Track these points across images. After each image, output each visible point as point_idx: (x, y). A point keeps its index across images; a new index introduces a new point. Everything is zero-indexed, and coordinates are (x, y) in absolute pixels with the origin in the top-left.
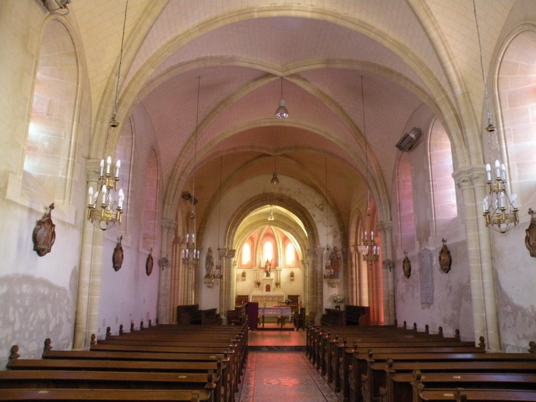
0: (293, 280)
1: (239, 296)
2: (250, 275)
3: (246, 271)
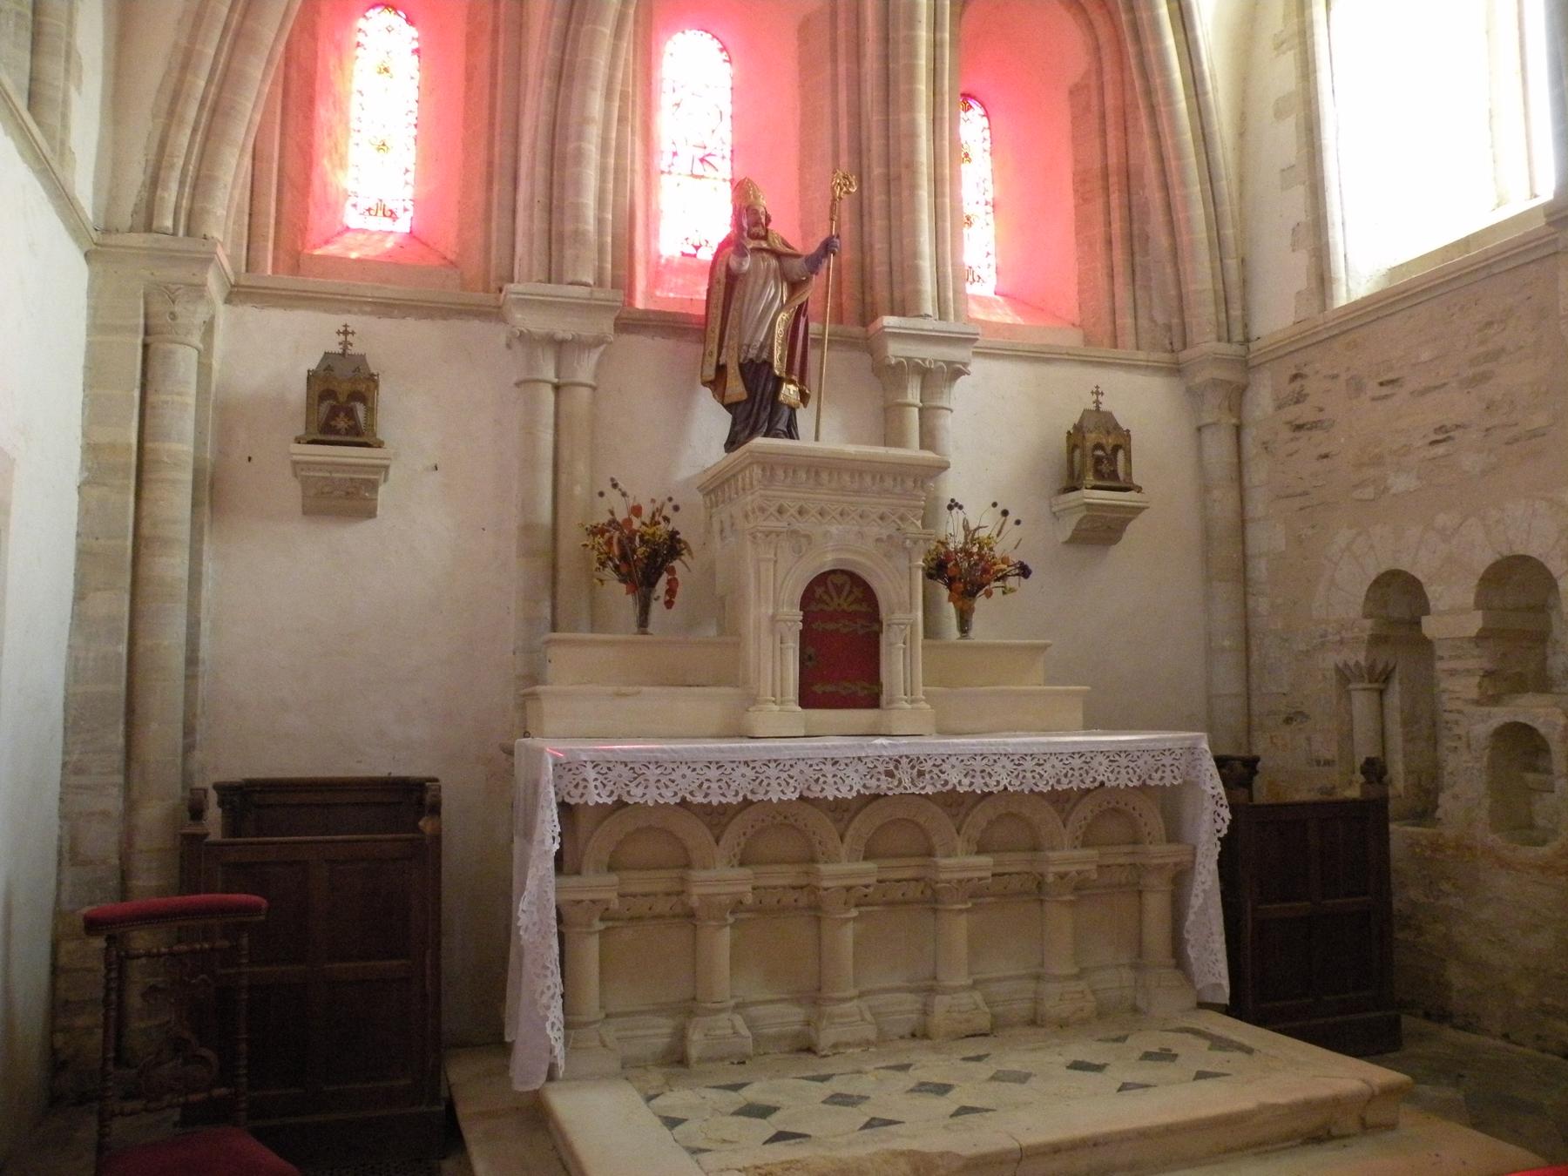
0: (1101, 532)
1: (251, 801)
2: (435, 407)
3: (382, 342)
